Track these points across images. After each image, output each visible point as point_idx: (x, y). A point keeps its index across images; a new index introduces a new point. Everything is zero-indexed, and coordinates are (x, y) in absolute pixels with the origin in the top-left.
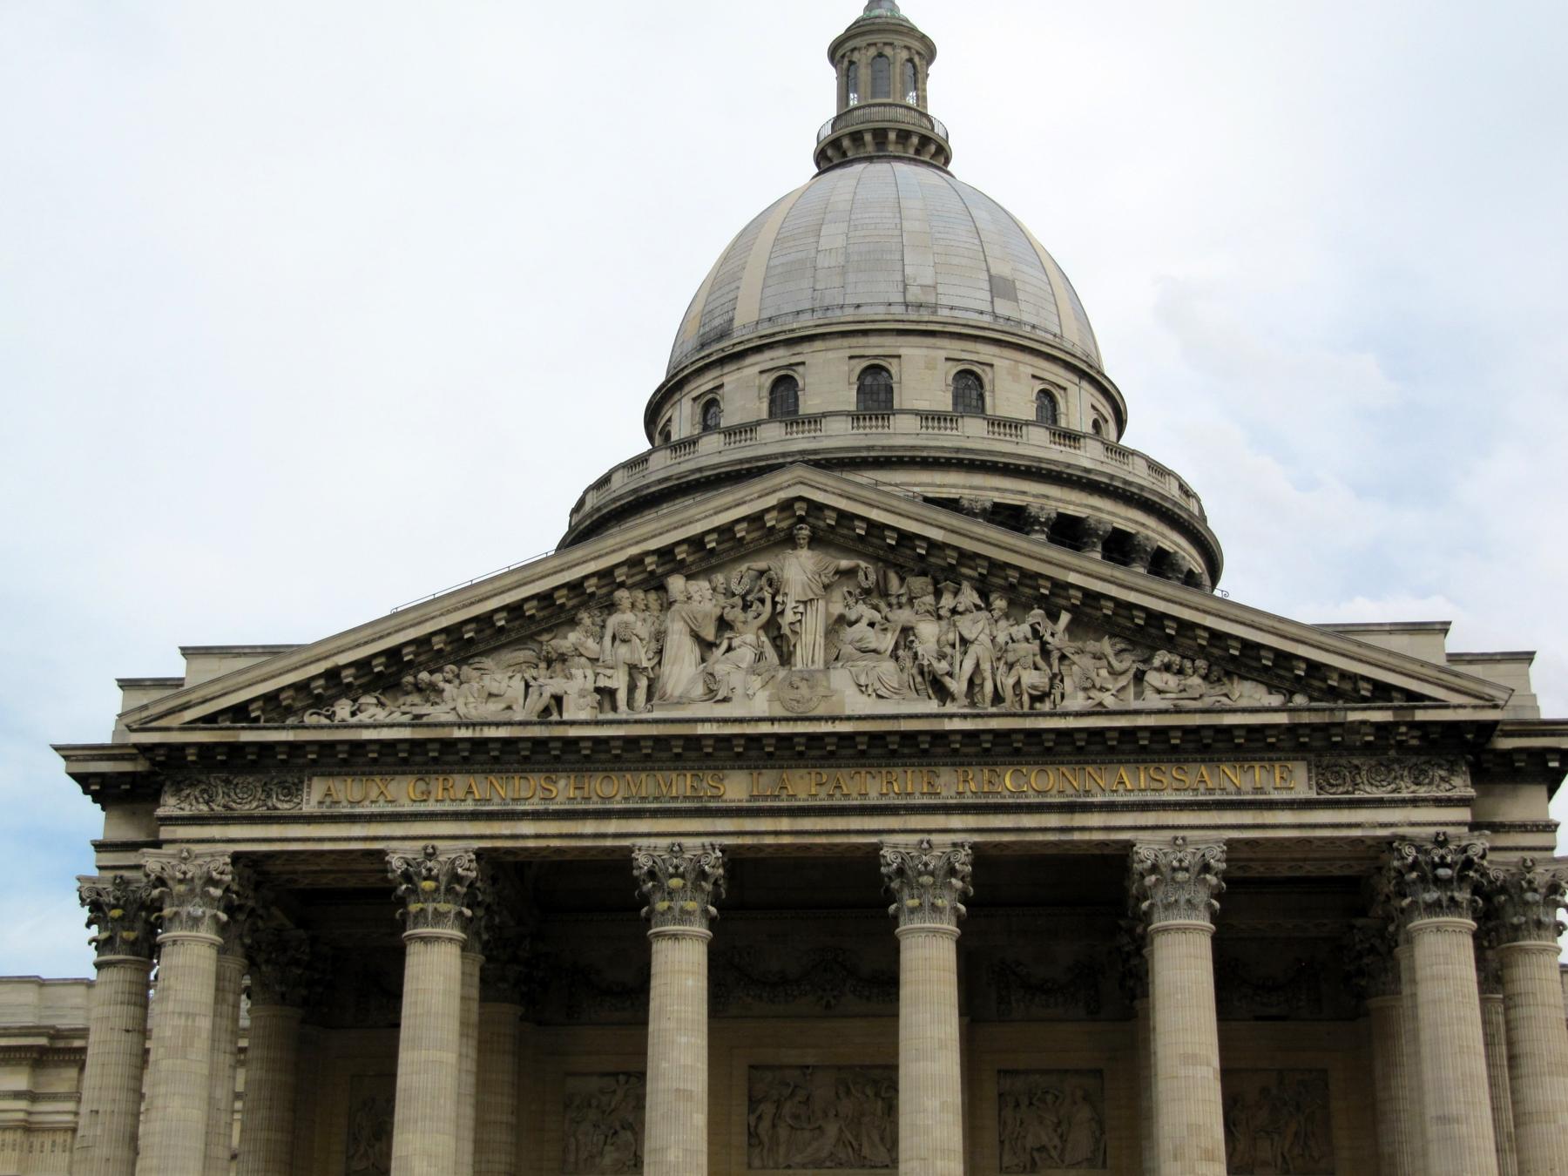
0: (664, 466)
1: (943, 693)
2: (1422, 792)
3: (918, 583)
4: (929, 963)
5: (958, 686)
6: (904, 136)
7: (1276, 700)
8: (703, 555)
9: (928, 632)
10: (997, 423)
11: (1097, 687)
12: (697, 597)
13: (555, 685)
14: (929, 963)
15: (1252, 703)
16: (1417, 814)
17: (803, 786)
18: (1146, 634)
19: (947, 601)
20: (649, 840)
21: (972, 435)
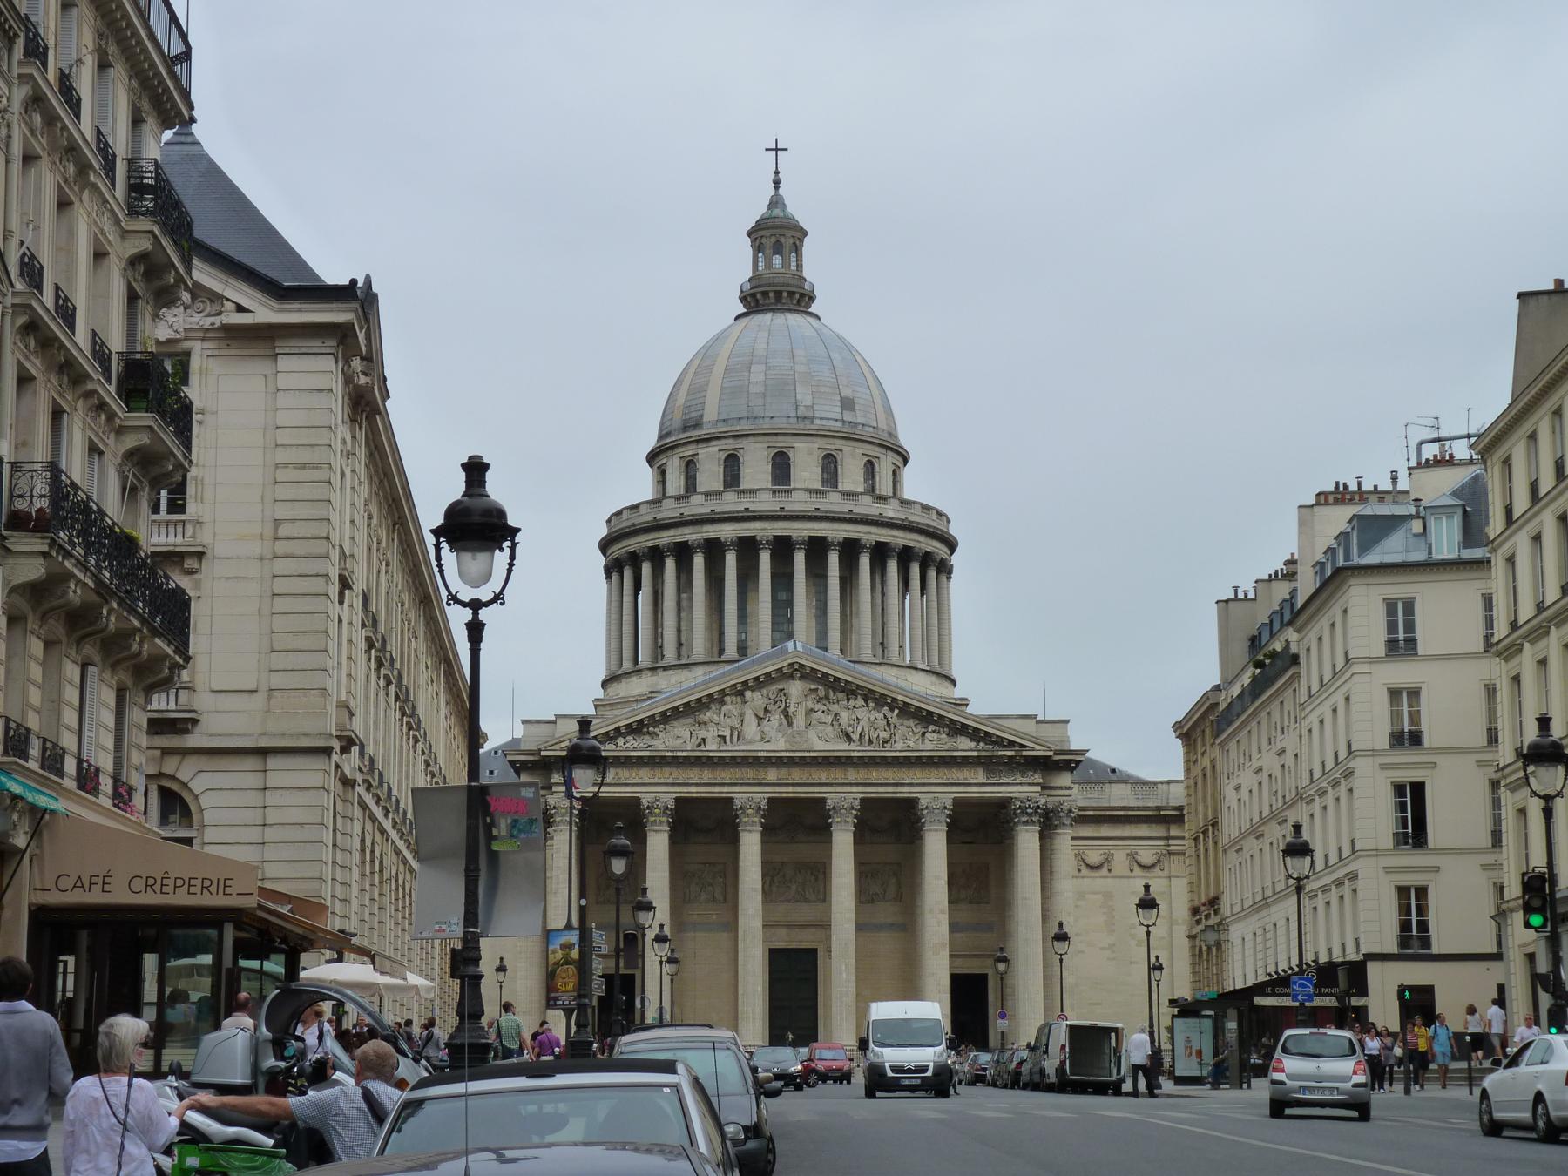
0: (669, 510)
1: (849, 738)
2: (1024, 780)
3: (841, 696)
4: (843, 842)
5: (855, 737)
6: (791, 294)
7: (973, 745)
8: (759, 683)
9: (844, 715)
10: (845, 494)
11: (908, 740)
12: (756, 699)
13: (702, 734)
14: (843, 842)
15: (965, 746)
16: (1021, 789)
17: (797, 775)
18: (926, 718)
19: (852, 703)
20: (740, 795)
21: (833, 503)
